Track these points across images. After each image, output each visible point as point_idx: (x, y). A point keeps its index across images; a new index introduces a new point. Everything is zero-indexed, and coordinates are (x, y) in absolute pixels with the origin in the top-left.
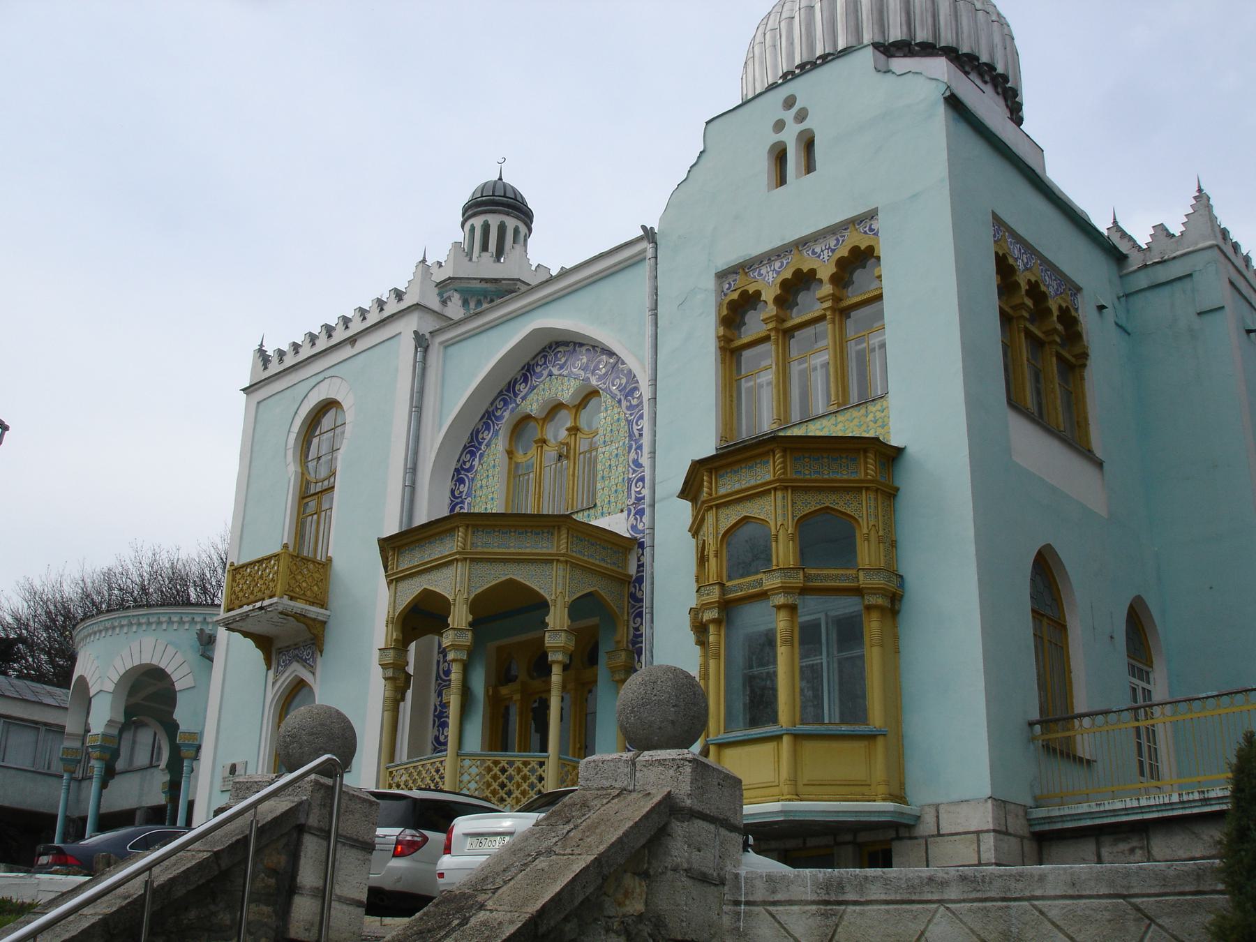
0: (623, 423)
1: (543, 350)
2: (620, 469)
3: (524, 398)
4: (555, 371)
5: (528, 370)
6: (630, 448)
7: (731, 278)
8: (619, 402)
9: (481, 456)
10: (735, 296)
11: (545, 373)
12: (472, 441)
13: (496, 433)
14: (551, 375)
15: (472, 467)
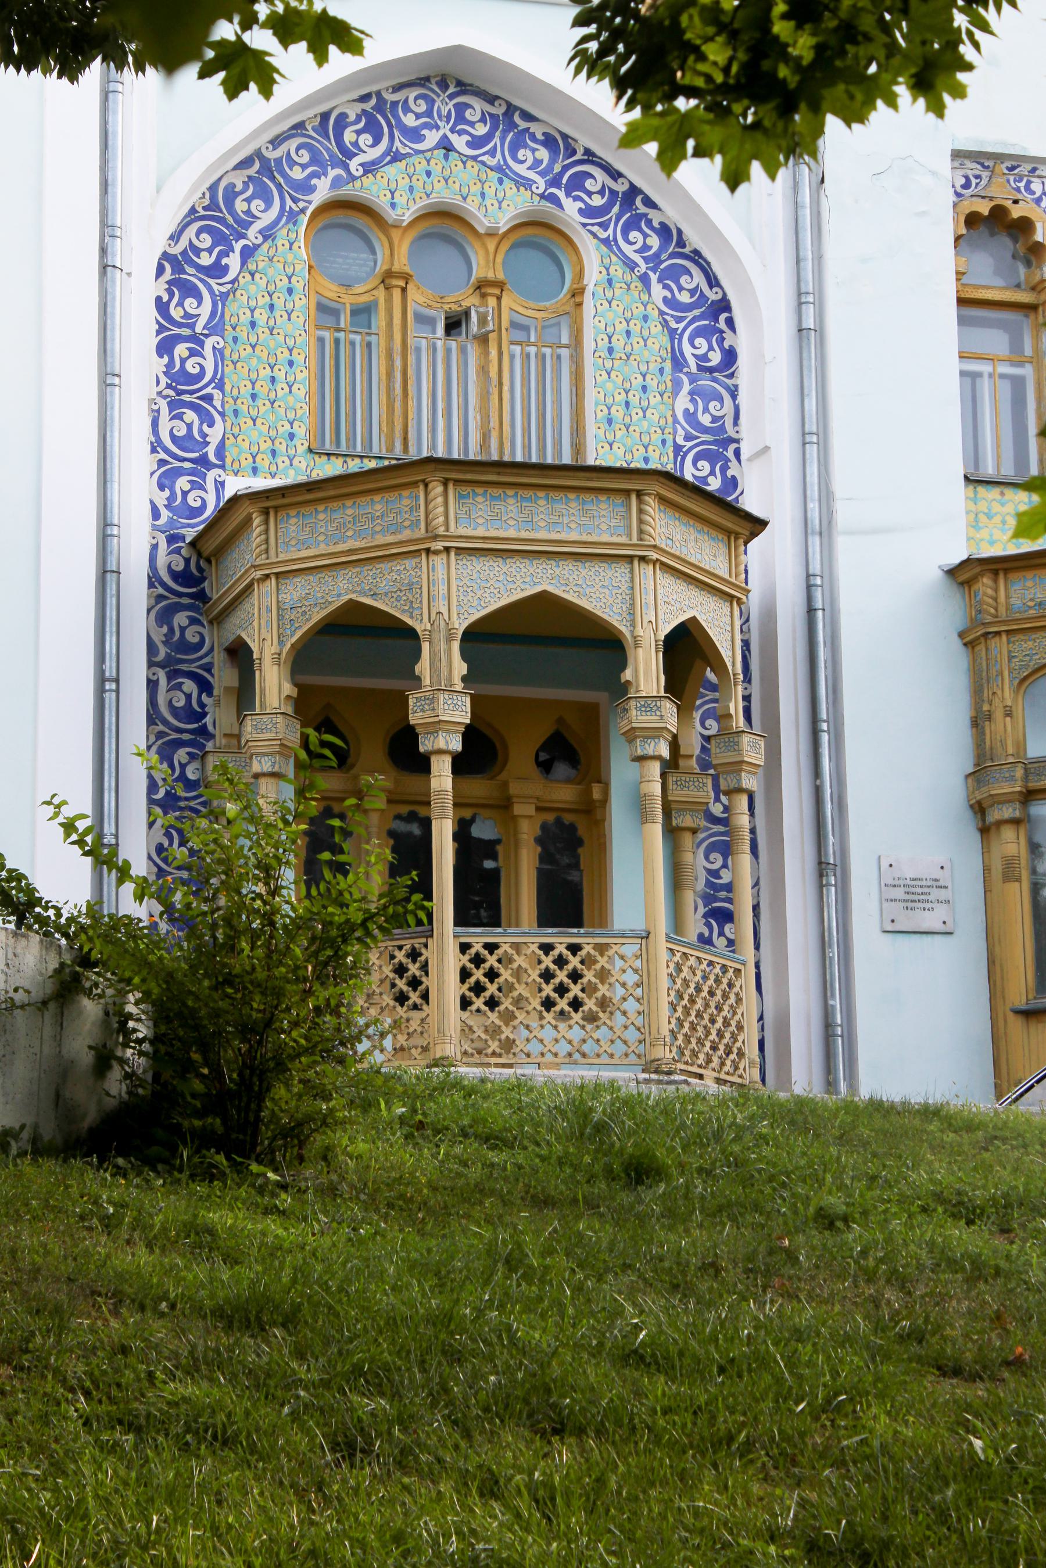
0: (656, 329)
1: (423, 81)
2: (653, 415)
3: (369, 168)
4: (459, 142)
5: (380, 107)
6: (677, 386)
7: (972, 168)
8: (645, 279)
9: (247, 253)
10: (984, 208)
11: (432, 138)
12: (213, 206)
13: (293, 217)
14: (446, 146)
15: (218, 270)
